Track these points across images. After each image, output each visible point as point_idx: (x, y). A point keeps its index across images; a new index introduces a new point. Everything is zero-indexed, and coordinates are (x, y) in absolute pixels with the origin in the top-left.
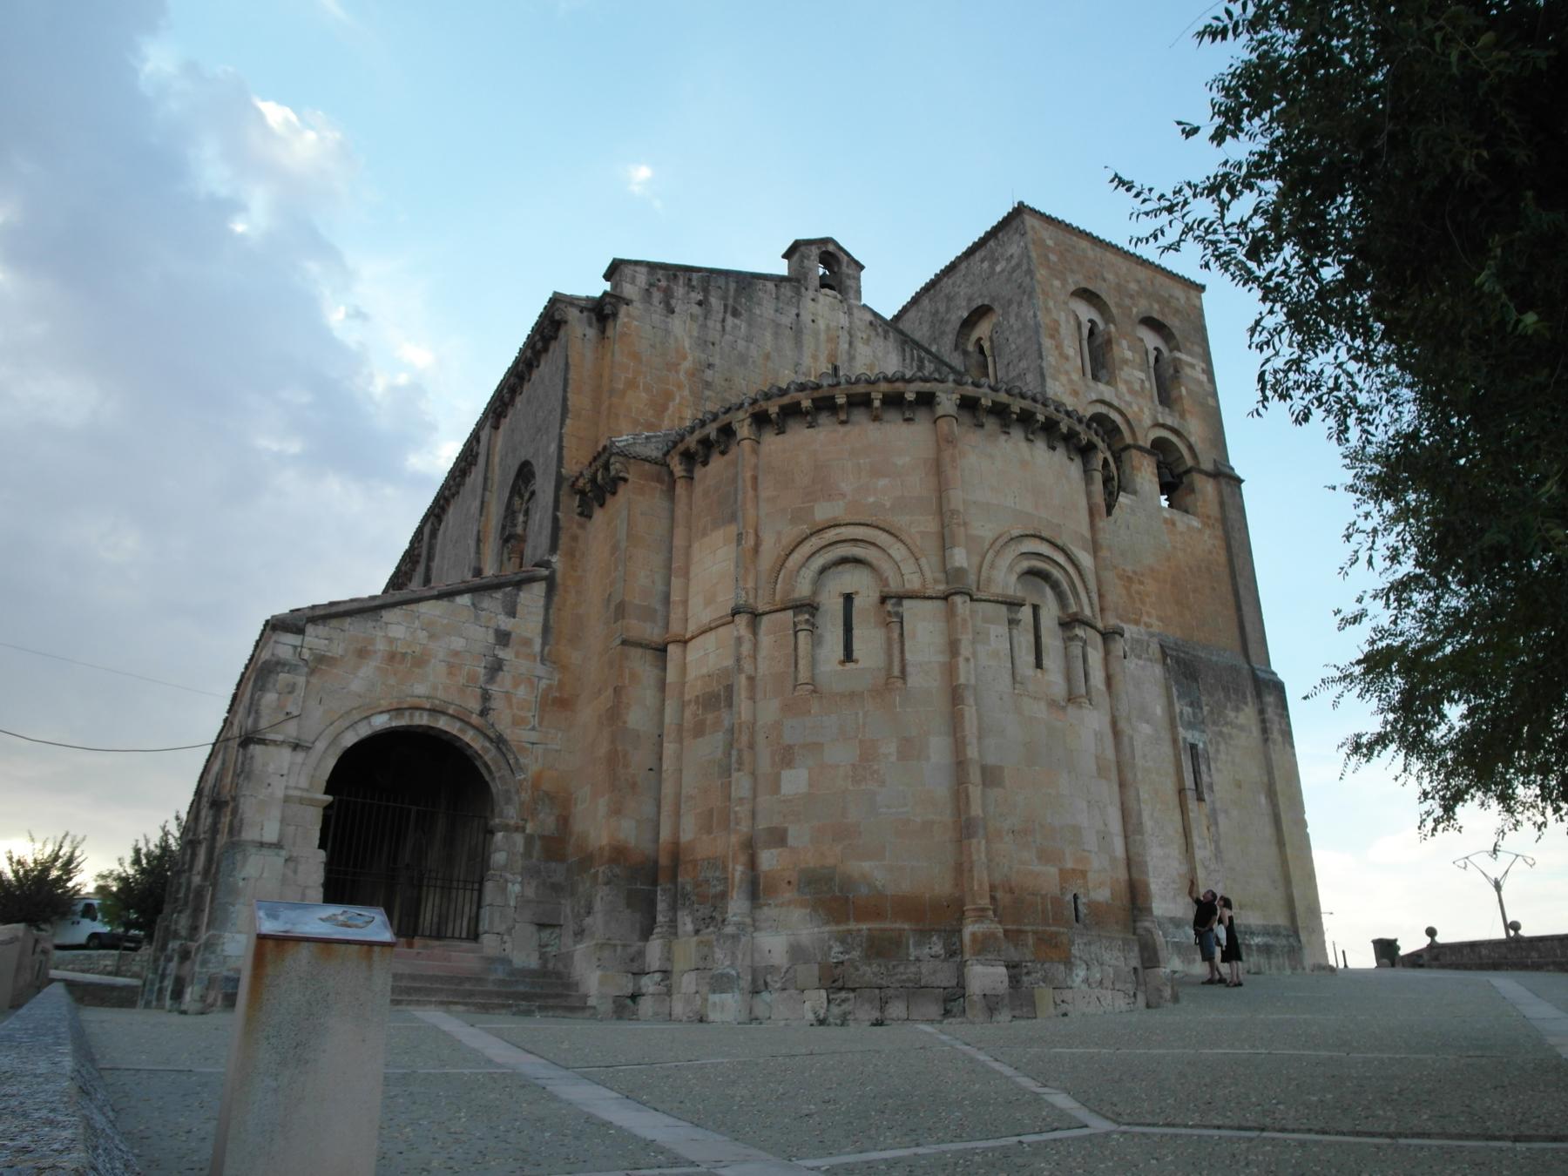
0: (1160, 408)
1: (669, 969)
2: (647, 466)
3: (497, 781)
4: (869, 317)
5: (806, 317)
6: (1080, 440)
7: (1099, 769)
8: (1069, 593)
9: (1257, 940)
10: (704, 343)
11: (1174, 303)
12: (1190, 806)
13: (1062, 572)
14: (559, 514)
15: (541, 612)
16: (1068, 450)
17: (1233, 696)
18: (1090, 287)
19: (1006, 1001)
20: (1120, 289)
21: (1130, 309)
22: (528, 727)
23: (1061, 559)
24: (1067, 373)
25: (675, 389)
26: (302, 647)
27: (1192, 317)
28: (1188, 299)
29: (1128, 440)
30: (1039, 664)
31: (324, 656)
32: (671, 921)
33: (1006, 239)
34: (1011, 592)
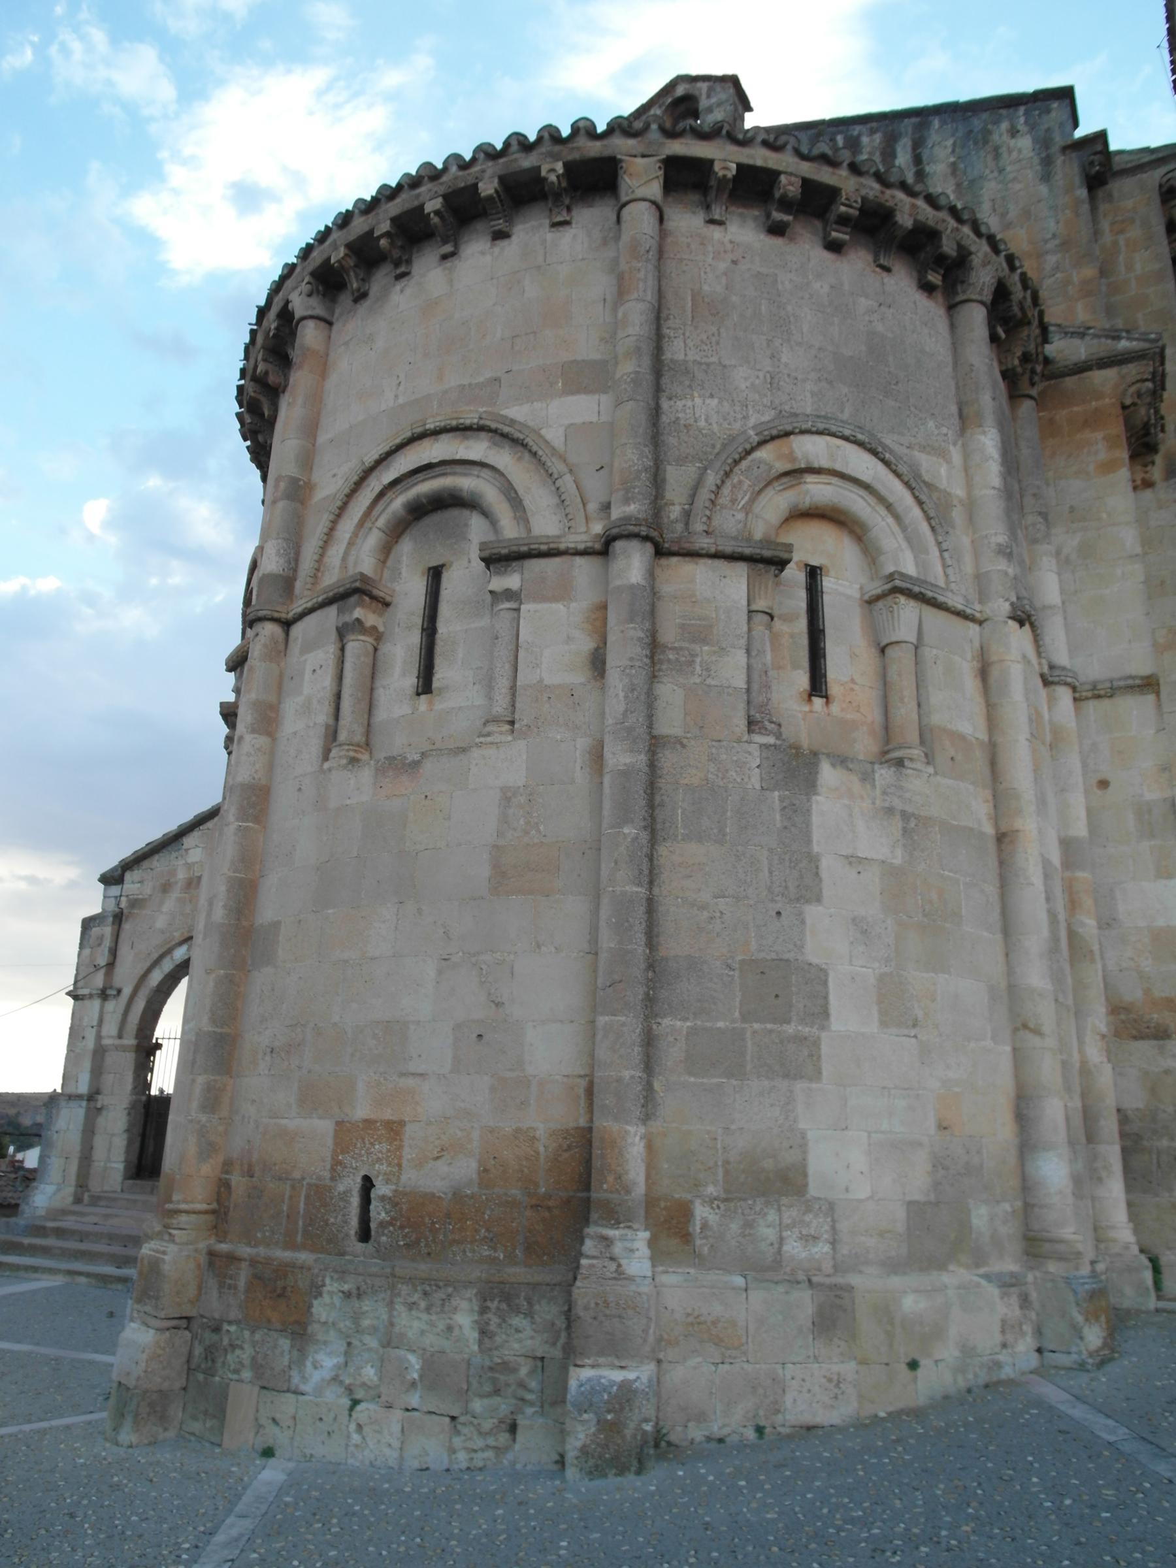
26: (121, 896)
31: (136, 900)
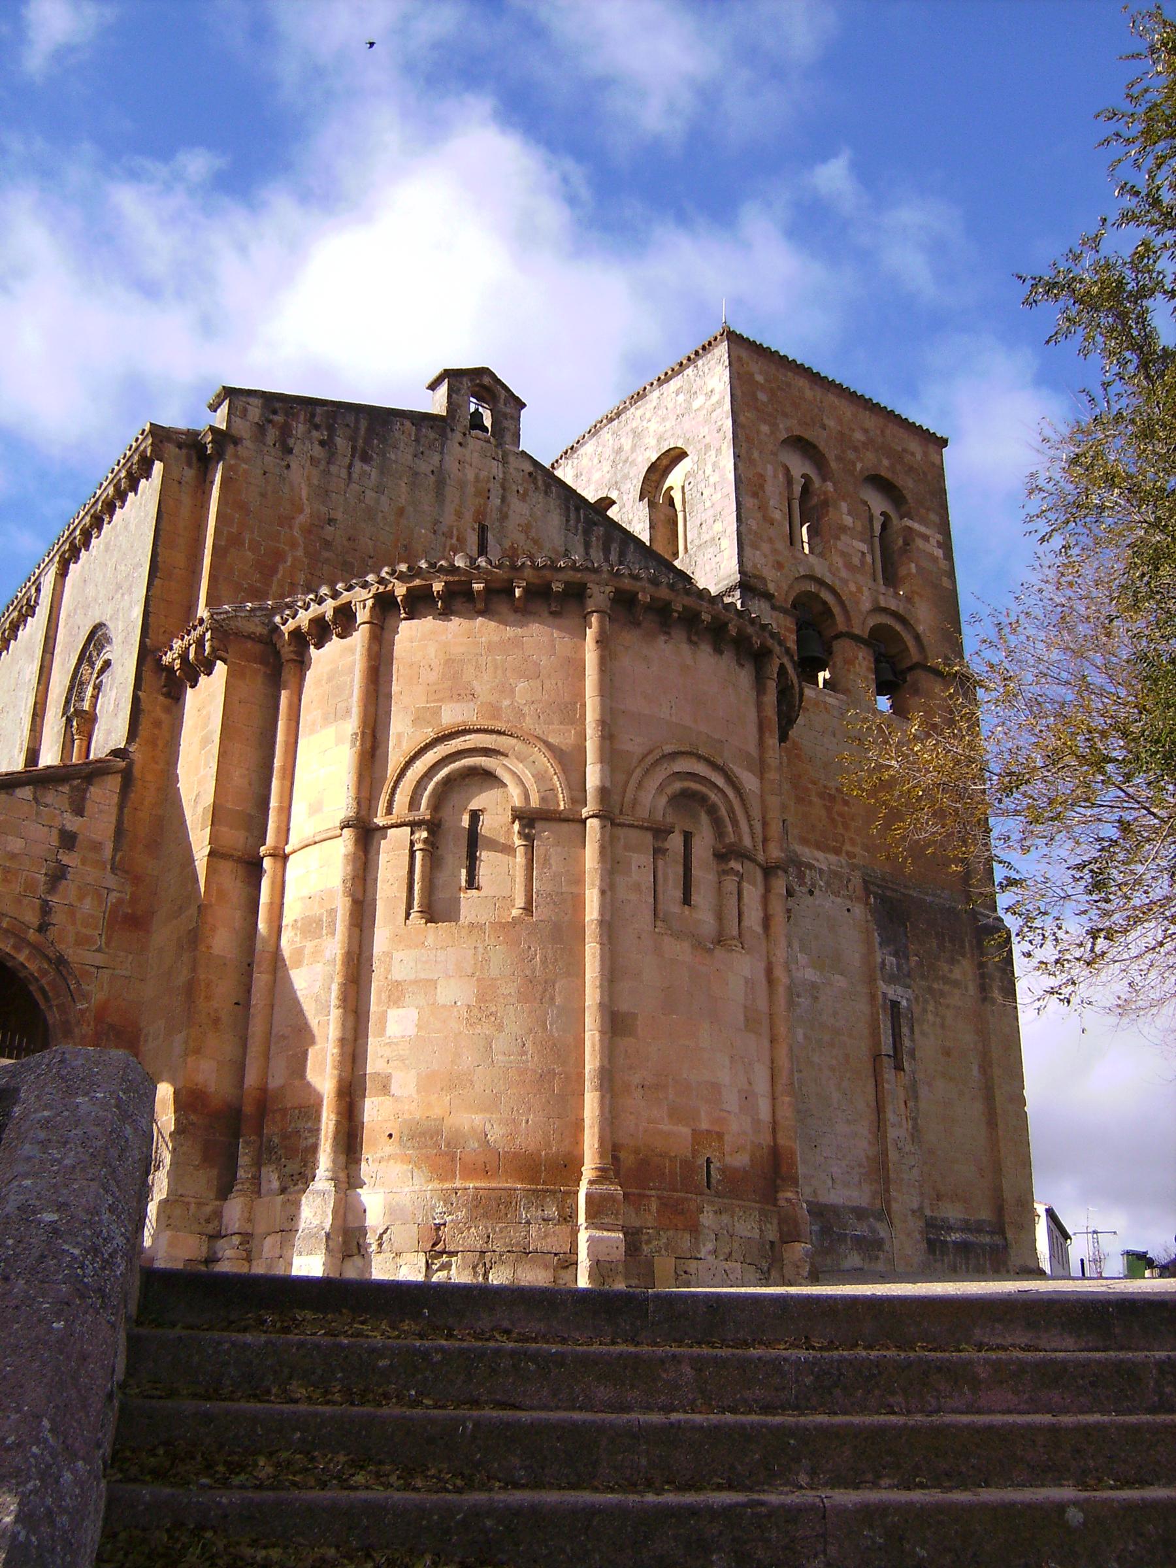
0: (883, 589)
1: (250, 1231)
2: (249, 644)
3: (55, 1009)
4: (529, 468)
5: (451, 465)
6: (751, 643)
7: (747, 1019)
8: (727, 819)
9: (955, 1236)
10: (323, 493)
11: (908, 458)
12: (886, 1076)
13: (719, 795)
14: (140, 693)
15: (114, 810)
16: (738, 654)
17: (947, 944)
18: (806, 436)
19: (621, 1268)
20: (843, 439)
21: (854, 464)
22: (94, 948)
23: (720, 781)
24: (770, 540)
25: (287, 548)
27: (929, 477)
28: (925, 454)
29: (842, 626)
30: (687, 900)
32: (253, 1177)
33: (706, 371)
34: (659, 816)
